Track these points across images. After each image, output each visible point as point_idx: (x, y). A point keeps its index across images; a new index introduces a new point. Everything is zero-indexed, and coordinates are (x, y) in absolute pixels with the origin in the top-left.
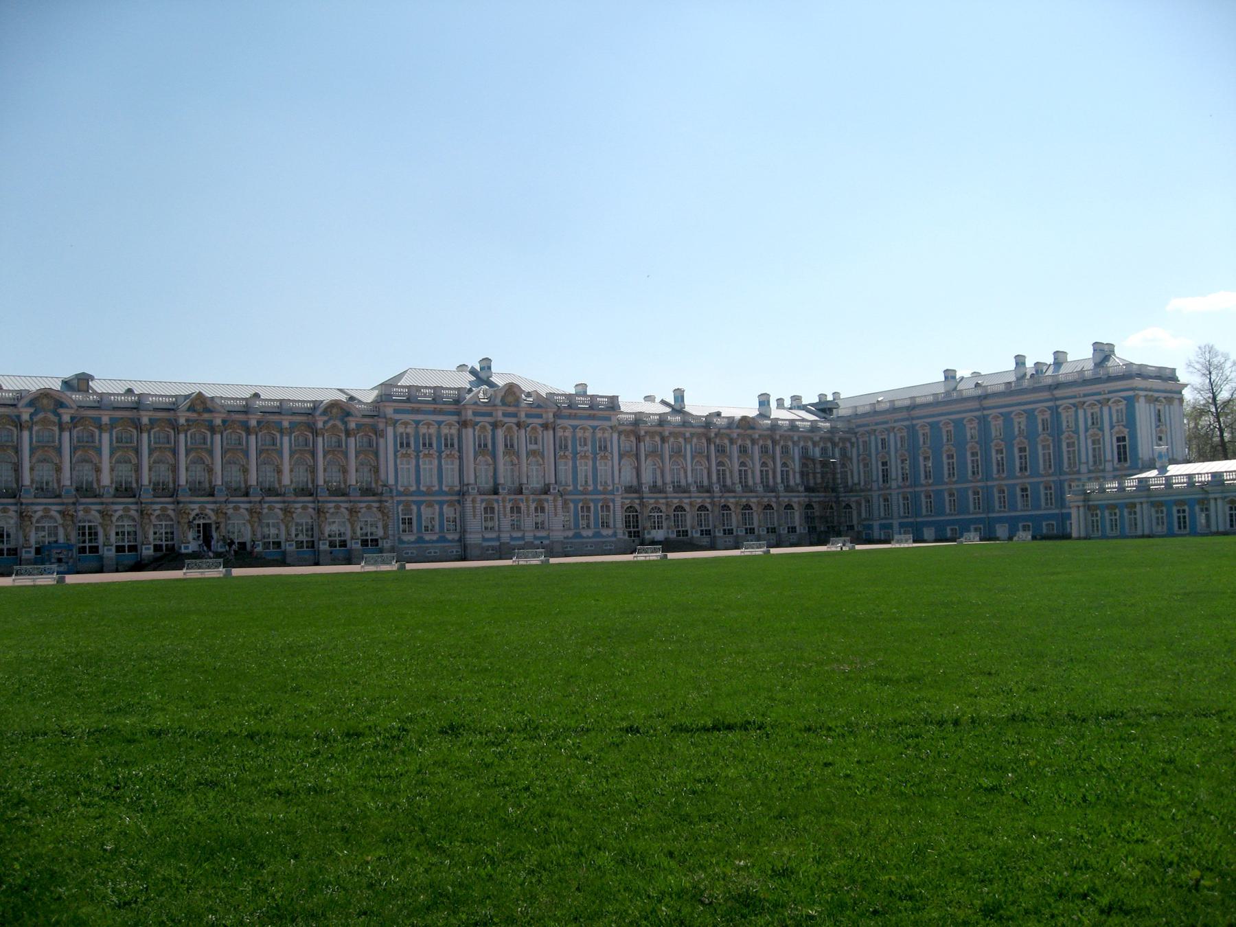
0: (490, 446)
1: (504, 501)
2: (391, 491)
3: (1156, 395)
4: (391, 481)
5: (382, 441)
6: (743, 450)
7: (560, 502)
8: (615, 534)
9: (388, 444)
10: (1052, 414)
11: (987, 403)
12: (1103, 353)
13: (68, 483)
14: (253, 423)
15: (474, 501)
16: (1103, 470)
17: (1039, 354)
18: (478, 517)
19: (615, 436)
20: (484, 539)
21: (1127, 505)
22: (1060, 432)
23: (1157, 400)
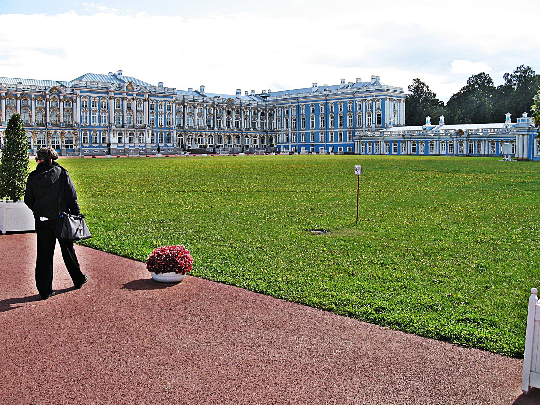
0: (121, 108)
1: (126, 131)
2: (79, 125)
3: (394, 98)
4: (79, 121)
5: (75, 104)
6: (228, 112)
7: (150, 132)
8: (173, 146)
9: (77, 106)
10: (353, 104)
11: (300, 100)
12: (377, 80)
13: (4, 120)
14: (19, 95)
15: (114, 131)
16: (371, 127)
17: (350, 79)
18: (116, 137)
19: (174, 105)
20: (118, 146)
21: (375, 142)
22: (356, 111)
23: (394, 100)
